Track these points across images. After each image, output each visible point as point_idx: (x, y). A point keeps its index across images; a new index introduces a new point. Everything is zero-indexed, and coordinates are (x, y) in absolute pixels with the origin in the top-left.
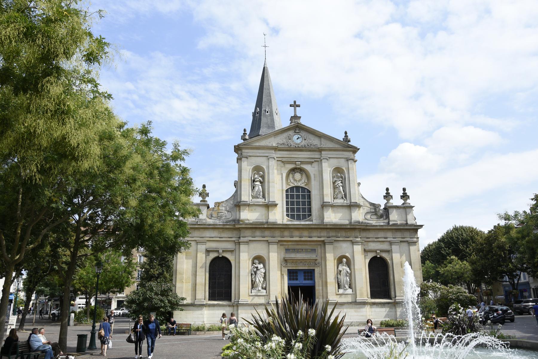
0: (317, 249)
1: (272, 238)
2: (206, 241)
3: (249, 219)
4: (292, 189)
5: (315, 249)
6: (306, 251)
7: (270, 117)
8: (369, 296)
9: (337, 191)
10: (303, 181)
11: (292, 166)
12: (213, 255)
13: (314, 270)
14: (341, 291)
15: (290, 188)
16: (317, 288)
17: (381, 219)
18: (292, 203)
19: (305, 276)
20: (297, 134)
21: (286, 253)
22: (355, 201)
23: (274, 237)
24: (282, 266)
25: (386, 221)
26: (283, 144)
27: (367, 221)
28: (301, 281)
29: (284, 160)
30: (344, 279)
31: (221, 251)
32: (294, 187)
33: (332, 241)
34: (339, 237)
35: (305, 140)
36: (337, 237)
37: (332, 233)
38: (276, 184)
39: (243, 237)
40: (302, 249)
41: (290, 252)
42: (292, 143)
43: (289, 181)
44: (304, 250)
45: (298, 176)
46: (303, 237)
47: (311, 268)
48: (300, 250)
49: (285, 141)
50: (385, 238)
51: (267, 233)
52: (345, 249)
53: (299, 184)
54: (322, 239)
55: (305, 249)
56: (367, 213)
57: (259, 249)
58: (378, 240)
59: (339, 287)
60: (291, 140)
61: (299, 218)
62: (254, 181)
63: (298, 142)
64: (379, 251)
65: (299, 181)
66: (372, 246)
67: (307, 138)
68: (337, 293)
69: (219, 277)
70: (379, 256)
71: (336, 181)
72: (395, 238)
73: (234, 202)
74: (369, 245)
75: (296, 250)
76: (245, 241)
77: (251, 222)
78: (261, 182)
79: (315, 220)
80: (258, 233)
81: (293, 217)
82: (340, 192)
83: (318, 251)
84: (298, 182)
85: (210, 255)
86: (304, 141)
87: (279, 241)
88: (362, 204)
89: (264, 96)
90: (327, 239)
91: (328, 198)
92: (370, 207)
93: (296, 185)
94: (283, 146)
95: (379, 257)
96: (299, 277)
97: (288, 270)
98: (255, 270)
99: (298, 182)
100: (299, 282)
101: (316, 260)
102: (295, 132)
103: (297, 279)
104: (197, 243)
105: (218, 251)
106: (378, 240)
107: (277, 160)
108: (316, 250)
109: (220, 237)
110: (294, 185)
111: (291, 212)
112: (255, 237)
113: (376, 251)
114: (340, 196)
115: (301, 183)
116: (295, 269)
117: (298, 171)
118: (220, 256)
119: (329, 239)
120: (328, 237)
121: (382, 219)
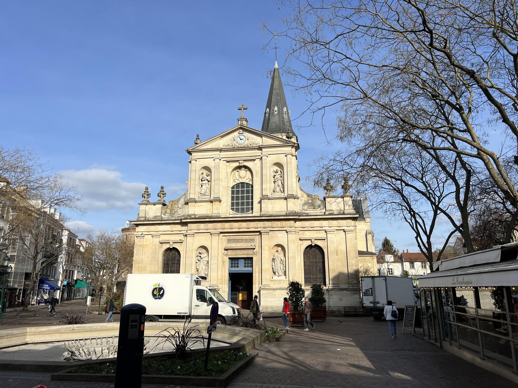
2: (159, 235)
3: (196, 214)
4: (237, 185)
6: (246, 241)
7: (278, 116)
9: (276, 184)
10: (247, 177)
11: (237, 164)
12: (166, 246)
14: (275, 278)
17: (318, 209)
18: (238, 198)
19: (245, 263)
20: (241, 135)
22: (292, 193)
23: (216, 229)
25: (324, 211)
26: (229, 145)
27: (304, 211)
28: (242, 268)
29: (228, 159)
30: (279, 266)
31: (171, 243)
32: (239, 183)
33: (267, 231)
35: (248, 140)
36: (272, 228)
37: (268, 224)
38: (222, 181)
39: (189, 230)
40: (243, 239)
42: (236, 144)
44: (244, 240)
45: (243, 172)
48: (240, 240)
49: (230, 142)
50: (320, 227)
51: (210, 225)
52: (281, 238)
53: (243, 181)
55: (245, 239)
56: (305, 204)
57: (203, 240)
58: (313, 229)
59: (274, 273)
60: (235, 141)
61: (243, 211)
62: (202, 181)
63: (242, 143)
65: (244, 178)
66: (308, 235)
67: (250, 138)
69: (171, 265)
70: (313, 245)
71: (275, 176)
72: (331, 227)
73: (185, 200)
74: (305, 234)
77: (197, 216)
78: (209, 181)
79: (256, 212)
80: (202, 226)
81: (237, 210)
82: (279, 186)
83: (256, 241)
84: (242, 179)
85: (163, 247)
86: (247, 141)
87: (221, 233)
88: (299, 195)
89: (273, 97)
90: (263, 229)
91: (268, 192)
92: (308, 198)
93: (241, 181)
94: (228, 147)
95: (313, 246)
97: (229, 258)
98: (199, 258)
99: (242, 179)
101: (254, 249)
102: (239, 134)
103: (238, 267)
104: (152, 236)
106: (313, 229)
109: (171, 231)
110: (239, 182)
111: (235, 205)
112: (199, 230)
113: (311, 240)
114: (278, 189)
115: (245, 179)
117: (242, 168)
118: (171, 247)
119: (265, 229)
120: (264, 228)
121: (319, 209)
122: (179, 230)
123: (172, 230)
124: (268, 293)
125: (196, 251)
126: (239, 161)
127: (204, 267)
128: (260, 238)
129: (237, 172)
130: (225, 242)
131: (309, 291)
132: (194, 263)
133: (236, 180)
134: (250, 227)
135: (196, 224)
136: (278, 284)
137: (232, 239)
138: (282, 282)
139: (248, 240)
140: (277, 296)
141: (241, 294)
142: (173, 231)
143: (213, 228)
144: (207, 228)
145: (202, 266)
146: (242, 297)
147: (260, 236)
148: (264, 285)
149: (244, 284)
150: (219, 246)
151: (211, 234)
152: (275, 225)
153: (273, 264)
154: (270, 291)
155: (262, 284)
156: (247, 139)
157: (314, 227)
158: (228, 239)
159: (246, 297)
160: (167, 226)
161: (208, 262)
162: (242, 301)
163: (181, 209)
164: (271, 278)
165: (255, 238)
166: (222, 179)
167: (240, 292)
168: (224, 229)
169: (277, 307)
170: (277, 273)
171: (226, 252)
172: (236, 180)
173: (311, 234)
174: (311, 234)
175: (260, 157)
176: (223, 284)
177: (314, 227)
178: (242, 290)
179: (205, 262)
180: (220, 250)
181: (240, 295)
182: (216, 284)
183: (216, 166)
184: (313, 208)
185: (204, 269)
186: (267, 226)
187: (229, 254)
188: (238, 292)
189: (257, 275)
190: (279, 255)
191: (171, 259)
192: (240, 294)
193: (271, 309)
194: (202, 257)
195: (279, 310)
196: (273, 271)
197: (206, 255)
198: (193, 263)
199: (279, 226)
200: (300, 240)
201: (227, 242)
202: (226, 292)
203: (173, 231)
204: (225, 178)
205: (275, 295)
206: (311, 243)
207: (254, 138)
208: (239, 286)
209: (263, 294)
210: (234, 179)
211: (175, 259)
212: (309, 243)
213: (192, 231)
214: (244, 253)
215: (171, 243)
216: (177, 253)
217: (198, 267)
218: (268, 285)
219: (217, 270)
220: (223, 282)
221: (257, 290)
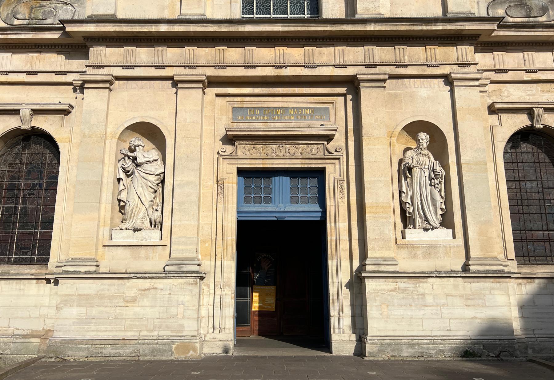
0: (334, 109)
1: (188, 71)
5: (328, 109)
6: (299, 113)
8: (512, 254)
13: (325, 167)
16: (330, 225)
21: (235, 119)
24: (221, 159)
31: (25, 112)
33: (382, 77)
34: (406, 66)
39: (94, 67)
40: (287, 109)
41: (247, 118)
44: (291, 112)
46: (286, 67)
47: (314, 164)
48: (278, 112)
54: (349, 71)
55: (294, 108)
58: (534, 76)
64: (541, 111)
68: (400, 240)
69: (26, 192)
75: (267, 112)
76: (99, 78)
83: (335, 114)
90: (363, 69)
95: (539, 130)
96: (274, 195)
98: (129, 164)
100: (274, 209)
101: (329, 138)
103: (268, 200)
105: (16, 112)
106: (534, 76)
108: (331, 111)
109: (29, 73)
112: (132, 67)
116: (261, 166)
118: (25, 127)
122: (58, 69)
123: (29, 70)
124: (394, 290)
125: (119, 138)
127: (147, 196)
128: (350, 104)
130: (224, 118)
131: (537, 281)
132: (109, 180)
134: (317, 62)
135: (122, 49)
136: (424, 258)
137: (249, 106)
138: (441, 249)
139: (307, 112)
140: (429, 299)
141: (257, 294)
142: (35, 73)
143: (182, 62)
144: (159, 61)
145: (140, 190)
146: (260, 301)
147: (349, 97)
148: (377, 259)
149: (265, 266)
150: (204, 128)
151: (175, 84)
152: (406, 58)
153: (404, 189)
154: (403, 284)
155: (364, 255)
157: (535, 71)
158: (236, 106)
159: (271, 301)
160: (15, 56)
161: (163, 182)
162: (261, 313)
163: (69, 7)
164: (399, 235)
165: (331, 106)
167: (255, 287)
168: (224, 67)
169: (433, 340)
170: (418, 221)
171: (229, 149)
173: (523, 94)
174: (523, 94)
176: (219, 255)
177: (535, 71)
178: (261, 283)
179: (153, 178)
180: (207, 141)
181: (256, 296)
182: (195, 255)
184: (524, 13)
185: (147, 204)
186: (377, 60)
187: (240, 154)
188: (249, 289)
189: (343, 225)
190: (421, 158)
191: (28, 172)
192: (254, 294)
193: (410, 350)
194: (139, 161)
195: (443, 351)
196: (403, 212)
197: (155, 154)
198: (105, 181)
199: (422, 60)
200: (492, 110)
201: (230, 115)
202: (229, 286)
203: (35, 73)
205: (424, 295)
206: (528, 123)
208: (253, 272)
209: (376, 293)
211: (42, 172)
212: (522, 121)
213: (106, 71)
214: (292, 152)
215: (25, 112)
216: (48, 153)
217: (123, 197)
218: (393, 259)
219: (196, 207)
220: (219, 251)
221: (346, 278)
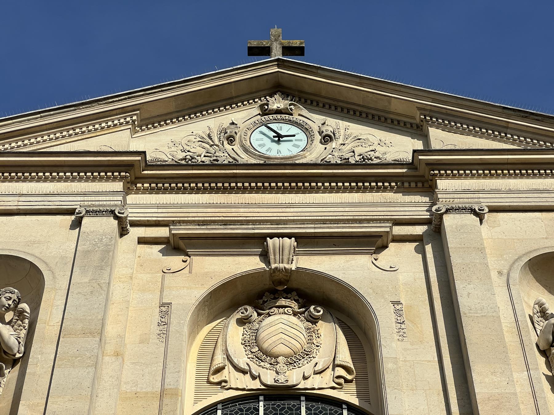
15: (225, 403)
38: (117, 354)
43: (219, 360)
93: (269, 378)
107: (142, 241)
110: (256, 385)
115: (308, 368)
126: (263, 238)
129: (241, 322)
133: (229, 374)
156: (318, 138)
166: (121, 337)
172: (229, 374)
175: (419, 230)
183: (87, 253)
204: (143, 341)
207: (371, 138)
210: (215, 366)
